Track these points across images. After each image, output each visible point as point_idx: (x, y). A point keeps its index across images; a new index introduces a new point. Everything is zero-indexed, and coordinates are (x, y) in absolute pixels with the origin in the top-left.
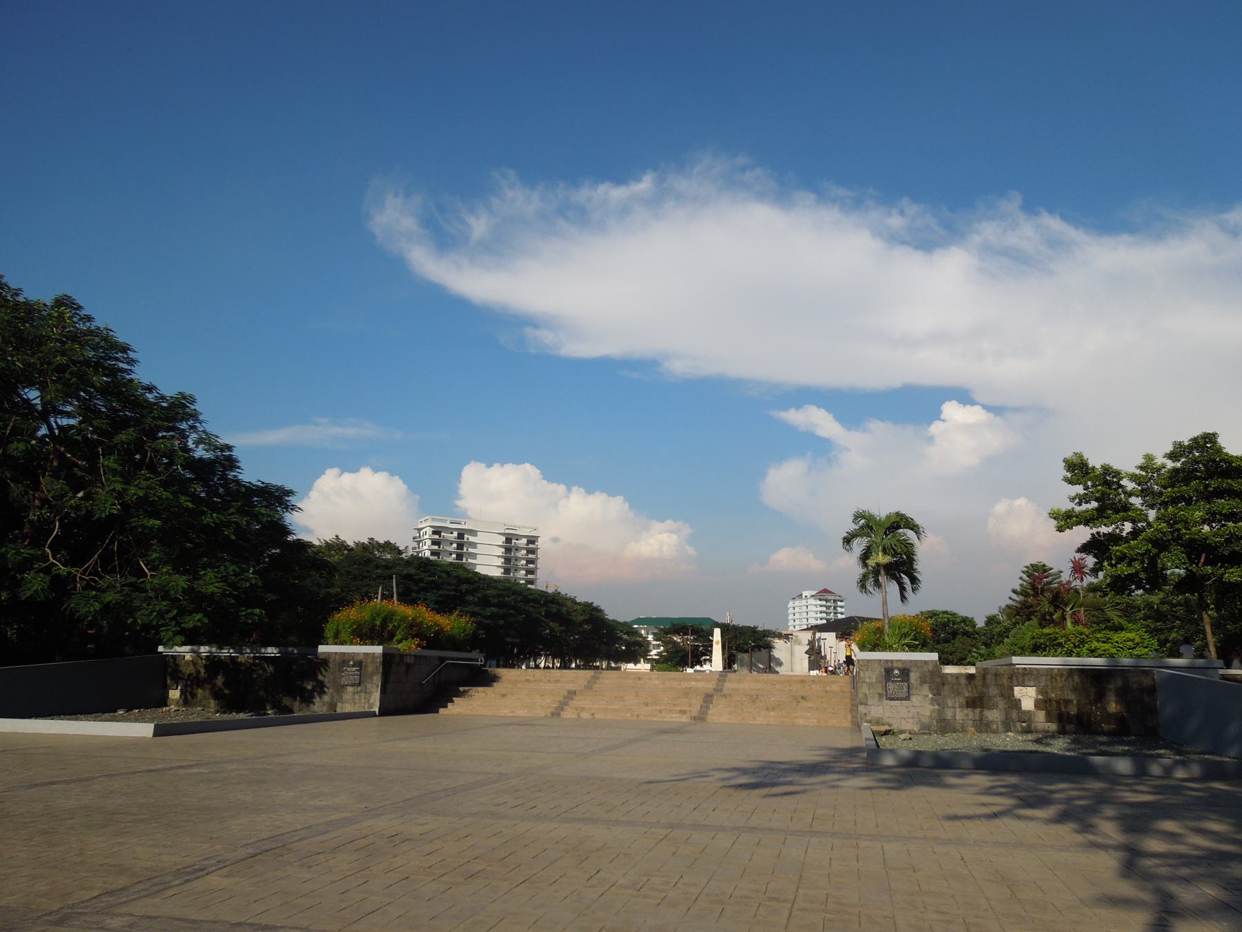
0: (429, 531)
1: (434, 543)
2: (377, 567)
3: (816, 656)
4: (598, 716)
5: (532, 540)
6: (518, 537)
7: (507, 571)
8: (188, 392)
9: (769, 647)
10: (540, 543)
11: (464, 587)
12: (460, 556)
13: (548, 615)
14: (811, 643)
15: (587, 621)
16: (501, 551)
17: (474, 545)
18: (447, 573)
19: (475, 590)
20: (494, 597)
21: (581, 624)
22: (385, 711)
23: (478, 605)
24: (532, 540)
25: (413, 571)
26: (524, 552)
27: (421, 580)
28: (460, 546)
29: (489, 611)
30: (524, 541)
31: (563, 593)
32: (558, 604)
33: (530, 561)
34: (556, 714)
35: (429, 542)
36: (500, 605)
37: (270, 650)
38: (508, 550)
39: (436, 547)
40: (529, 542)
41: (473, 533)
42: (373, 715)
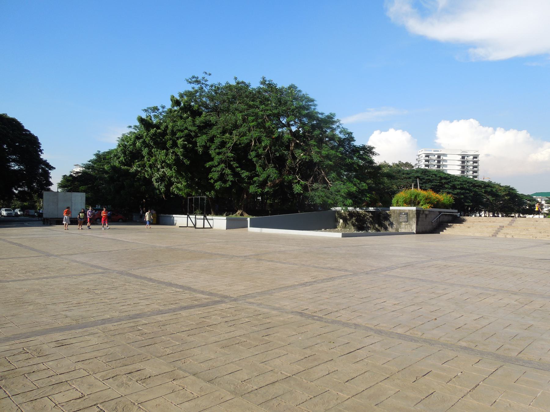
0: (424, 155)
1: (426, 161)
2: (403, 174)
4: (515, 237)
5: (475, 157)
7: (463, 172)
8: (333, 112)
10: (480, 158)
11: (444, 181)
12: (439, 167)
13: (486, 192)
15: (507, 195)
17: (445, 161)
18: (436, 175)
19: (449, 182)
20: (458, 185)
21: (503, 196)
22: (418, 232)
23: (450, 189)
24: (475, 157)
25: (419, 175)
27: (424, 179)
29: (456, 191)
30: (472, 157)
31: (493, 181)
32: (491, 187)
33: (476, 167)
34: (494, 235)
35: (424, 161)
36: (462, 189)
37: (370, 208)
38: (463, 162)
39: (427, 163)
41: (445, 155)
42: (414, 233)
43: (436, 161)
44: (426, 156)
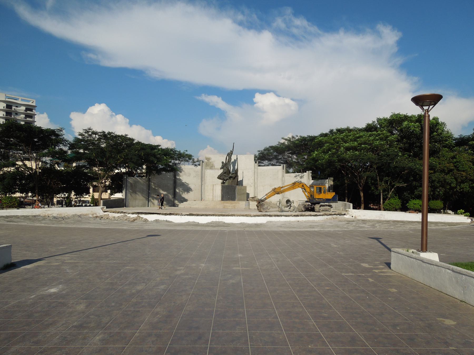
3: (231, 183)
6: (18, 105)
9: (174, 170)
14: (225, 166)
24: (29, 108)
26: (23, 116)
30: (23, 108)
40: (27, 110)
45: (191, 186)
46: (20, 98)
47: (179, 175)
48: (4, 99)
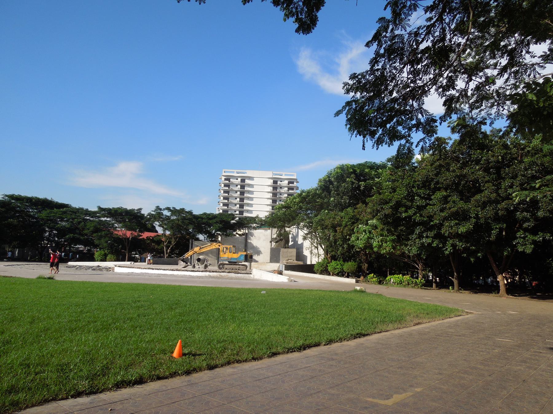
0: (223, 178)
1: (225, 186)
16: (270, 189)
17: (251, 186)
24: (291, 182)
28: (243, 187)
38: (275, 188)
40: (289, 183)
43: (239, 186)
44: (225, 179)
45: (262, 249)
46: (284, 173)
47: (250, 239)
48: (271, 177)
